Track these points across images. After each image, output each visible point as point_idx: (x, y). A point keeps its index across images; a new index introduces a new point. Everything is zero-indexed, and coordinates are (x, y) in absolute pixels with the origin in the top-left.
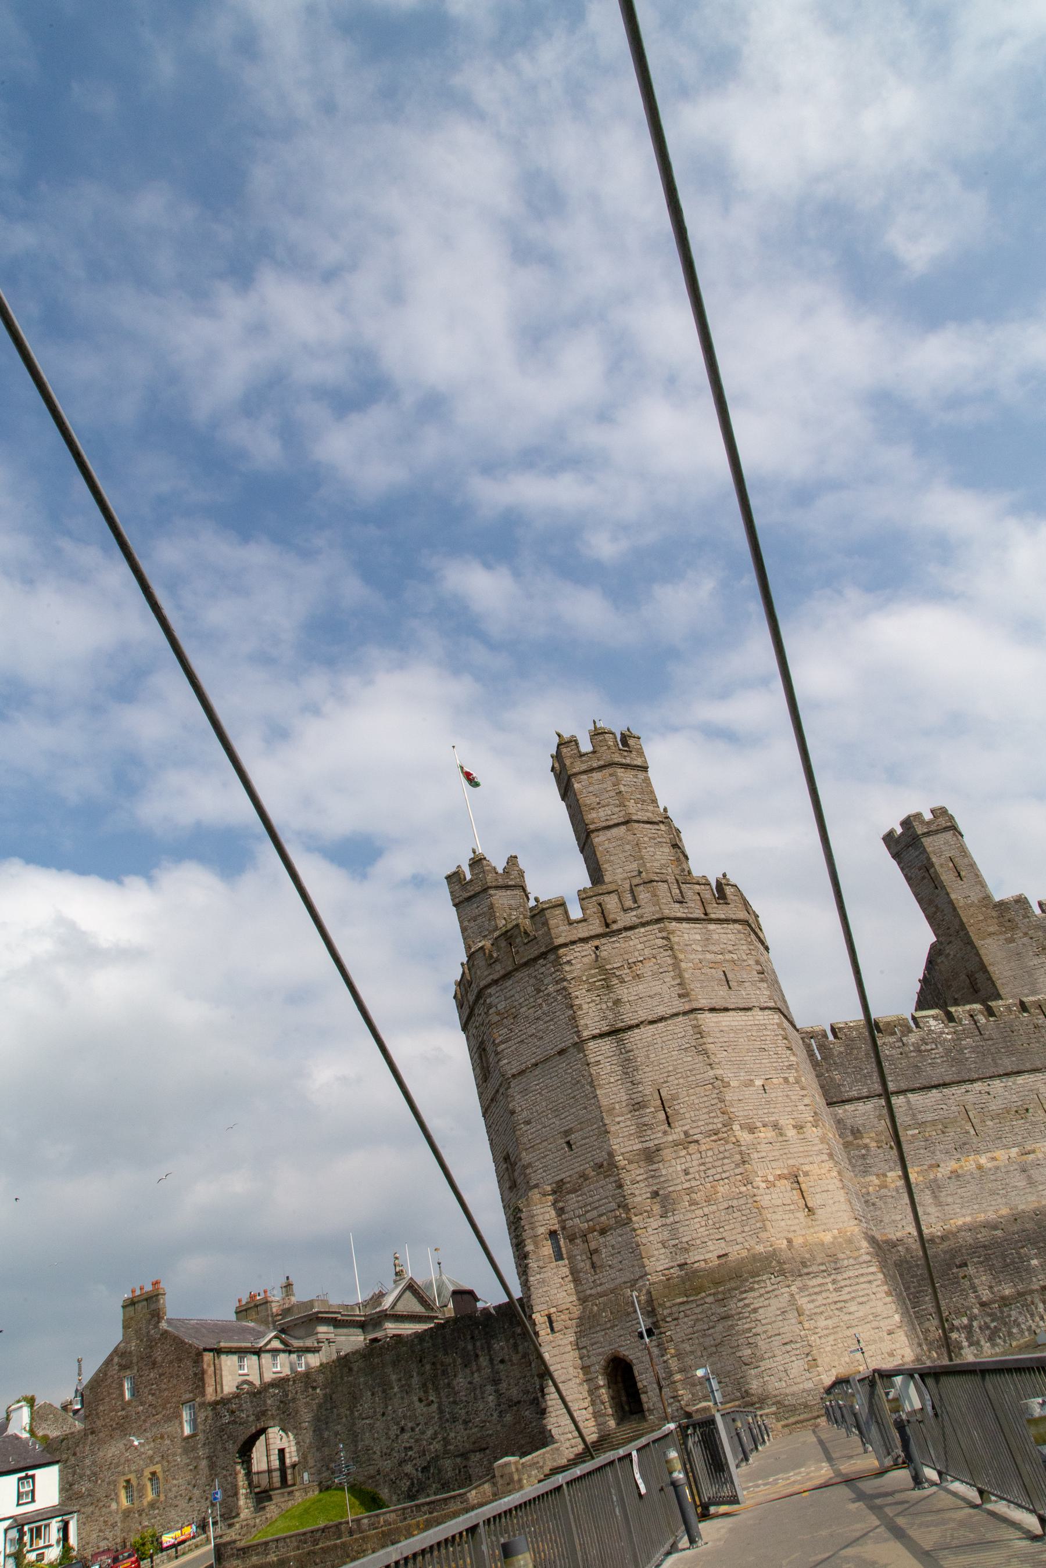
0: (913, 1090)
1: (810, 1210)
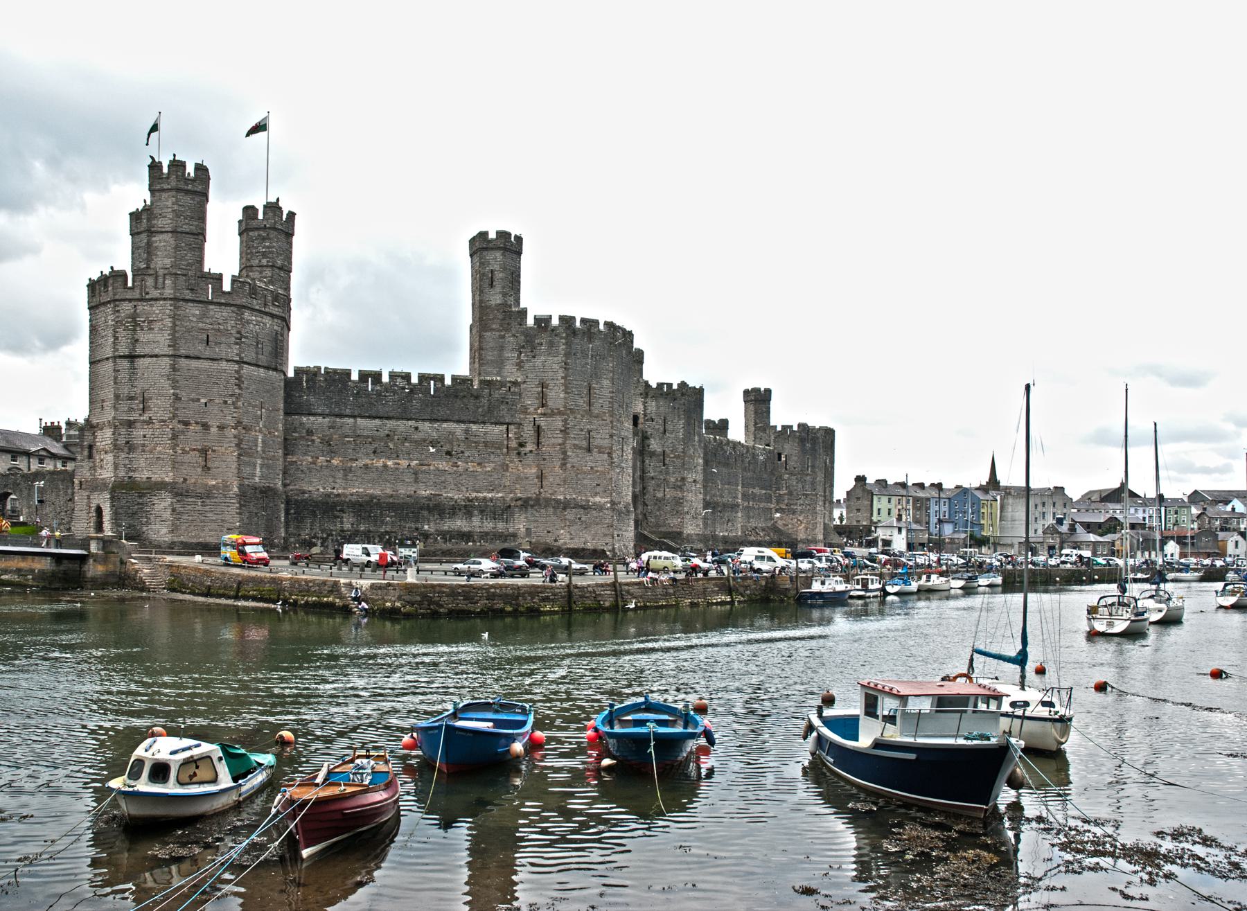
0: (362, 417)
1: (206, 468)
